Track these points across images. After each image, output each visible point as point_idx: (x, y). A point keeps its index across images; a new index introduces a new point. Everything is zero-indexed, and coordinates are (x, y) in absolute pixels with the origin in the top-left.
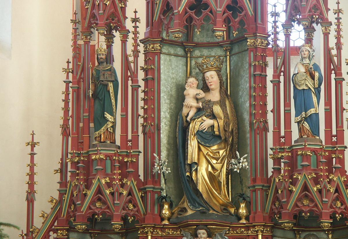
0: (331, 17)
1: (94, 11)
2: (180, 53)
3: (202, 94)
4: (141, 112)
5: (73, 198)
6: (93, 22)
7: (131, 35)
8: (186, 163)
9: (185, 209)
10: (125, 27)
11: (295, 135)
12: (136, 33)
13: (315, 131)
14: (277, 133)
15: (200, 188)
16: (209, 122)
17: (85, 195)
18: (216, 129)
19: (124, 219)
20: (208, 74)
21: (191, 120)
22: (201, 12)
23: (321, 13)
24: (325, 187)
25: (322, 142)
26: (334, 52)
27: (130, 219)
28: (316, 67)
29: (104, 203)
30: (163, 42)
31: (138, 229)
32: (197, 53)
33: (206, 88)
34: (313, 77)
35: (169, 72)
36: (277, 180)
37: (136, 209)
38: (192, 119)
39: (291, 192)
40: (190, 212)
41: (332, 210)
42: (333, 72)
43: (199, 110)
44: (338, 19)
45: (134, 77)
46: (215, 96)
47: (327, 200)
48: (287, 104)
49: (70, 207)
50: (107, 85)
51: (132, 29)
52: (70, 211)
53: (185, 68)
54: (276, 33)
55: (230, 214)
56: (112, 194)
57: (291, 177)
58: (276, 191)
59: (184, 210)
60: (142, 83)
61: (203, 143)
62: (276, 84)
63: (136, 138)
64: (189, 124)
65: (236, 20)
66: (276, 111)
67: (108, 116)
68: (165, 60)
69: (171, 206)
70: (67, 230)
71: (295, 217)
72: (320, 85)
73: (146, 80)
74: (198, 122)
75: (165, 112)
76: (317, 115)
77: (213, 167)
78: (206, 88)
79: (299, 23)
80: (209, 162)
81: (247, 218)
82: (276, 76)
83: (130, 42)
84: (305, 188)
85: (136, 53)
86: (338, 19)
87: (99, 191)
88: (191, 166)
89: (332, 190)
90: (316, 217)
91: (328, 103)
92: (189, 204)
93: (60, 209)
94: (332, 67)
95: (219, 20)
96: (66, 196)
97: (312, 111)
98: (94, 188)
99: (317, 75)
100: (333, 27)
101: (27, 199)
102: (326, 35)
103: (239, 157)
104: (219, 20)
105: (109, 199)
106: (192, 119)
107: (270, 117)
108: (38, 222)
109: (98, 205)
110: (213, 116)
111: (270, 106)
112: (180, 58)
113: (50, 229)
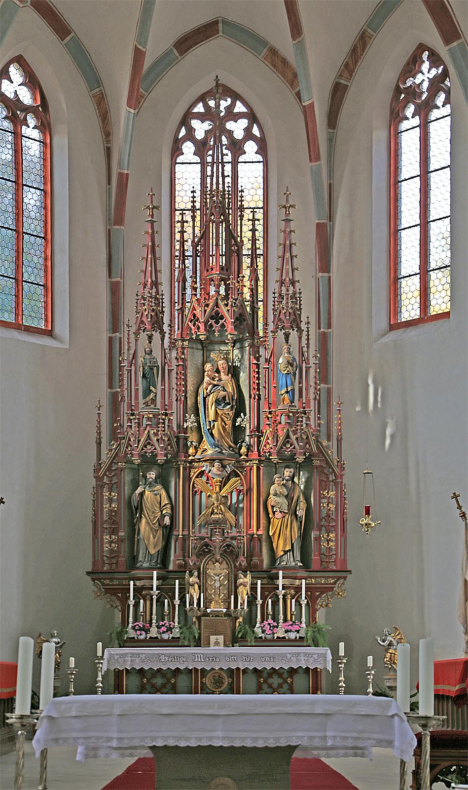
0: (303, 326)
1: (143, 319)
2: (199, 348)
3: (217, 375)
4: (175, 386)
5: (130, 442)
6: (142, 326)
7: (167, 336)
8: (207, 420)
9: (206, 449)
10: (164, 330)
13: (292, 402)
17: (139, 441)
18: (227, 398)
19: (166, 455)
20: (220, 362)
21: (210, 392)
22: (219, 322)
23: (298, 324)
24: (301, 435)
25: (296, 407)
26: (305, 349)
27: (169, 456)
28: (294, 359)
31: (174, 462)
32: (210, 347)
33: (218, 371)
34: (292, 366)
35: (192, 360)
36: (269, 431)
37: (171, 450)
40: (210, 452)
41: (304, 450)
42: (304, 362)
44: (308, 328)
47: (302, 444)
49: (127, 447)
50: (152, 369)
51: (168, 332)
52: (127, 450)
53: (202, 357)
55: (236, 453)
56: (158, 440)
59: (205, 450)
60: (175, 368)
61: (219, 407)
63: (171, 403)
65: (241, 327)
67: (152, 388)
68: (190, 352)
69: (196, 448)
70: (125, 462)
72: (296, 370)
75: (190, 387)
76: (293, 390)
77: (225, 423)
79: (281, 330)
81: (247, 455)
83: (167, 340)
84: (288, 436)
86: (308, 328)
89: (305, 437)
92: (209, 447)
93: (120, 448)
94: (303, 359)
96: (124, 441)
99: (295, 363)
100: (305, 333)
101: (96, 442)
102: (300, 338)
103: (243, 417)
105: (156, 443)
109: (149, 447)
110: (224, 390)
112: (199, 351)
113: (111, 463)
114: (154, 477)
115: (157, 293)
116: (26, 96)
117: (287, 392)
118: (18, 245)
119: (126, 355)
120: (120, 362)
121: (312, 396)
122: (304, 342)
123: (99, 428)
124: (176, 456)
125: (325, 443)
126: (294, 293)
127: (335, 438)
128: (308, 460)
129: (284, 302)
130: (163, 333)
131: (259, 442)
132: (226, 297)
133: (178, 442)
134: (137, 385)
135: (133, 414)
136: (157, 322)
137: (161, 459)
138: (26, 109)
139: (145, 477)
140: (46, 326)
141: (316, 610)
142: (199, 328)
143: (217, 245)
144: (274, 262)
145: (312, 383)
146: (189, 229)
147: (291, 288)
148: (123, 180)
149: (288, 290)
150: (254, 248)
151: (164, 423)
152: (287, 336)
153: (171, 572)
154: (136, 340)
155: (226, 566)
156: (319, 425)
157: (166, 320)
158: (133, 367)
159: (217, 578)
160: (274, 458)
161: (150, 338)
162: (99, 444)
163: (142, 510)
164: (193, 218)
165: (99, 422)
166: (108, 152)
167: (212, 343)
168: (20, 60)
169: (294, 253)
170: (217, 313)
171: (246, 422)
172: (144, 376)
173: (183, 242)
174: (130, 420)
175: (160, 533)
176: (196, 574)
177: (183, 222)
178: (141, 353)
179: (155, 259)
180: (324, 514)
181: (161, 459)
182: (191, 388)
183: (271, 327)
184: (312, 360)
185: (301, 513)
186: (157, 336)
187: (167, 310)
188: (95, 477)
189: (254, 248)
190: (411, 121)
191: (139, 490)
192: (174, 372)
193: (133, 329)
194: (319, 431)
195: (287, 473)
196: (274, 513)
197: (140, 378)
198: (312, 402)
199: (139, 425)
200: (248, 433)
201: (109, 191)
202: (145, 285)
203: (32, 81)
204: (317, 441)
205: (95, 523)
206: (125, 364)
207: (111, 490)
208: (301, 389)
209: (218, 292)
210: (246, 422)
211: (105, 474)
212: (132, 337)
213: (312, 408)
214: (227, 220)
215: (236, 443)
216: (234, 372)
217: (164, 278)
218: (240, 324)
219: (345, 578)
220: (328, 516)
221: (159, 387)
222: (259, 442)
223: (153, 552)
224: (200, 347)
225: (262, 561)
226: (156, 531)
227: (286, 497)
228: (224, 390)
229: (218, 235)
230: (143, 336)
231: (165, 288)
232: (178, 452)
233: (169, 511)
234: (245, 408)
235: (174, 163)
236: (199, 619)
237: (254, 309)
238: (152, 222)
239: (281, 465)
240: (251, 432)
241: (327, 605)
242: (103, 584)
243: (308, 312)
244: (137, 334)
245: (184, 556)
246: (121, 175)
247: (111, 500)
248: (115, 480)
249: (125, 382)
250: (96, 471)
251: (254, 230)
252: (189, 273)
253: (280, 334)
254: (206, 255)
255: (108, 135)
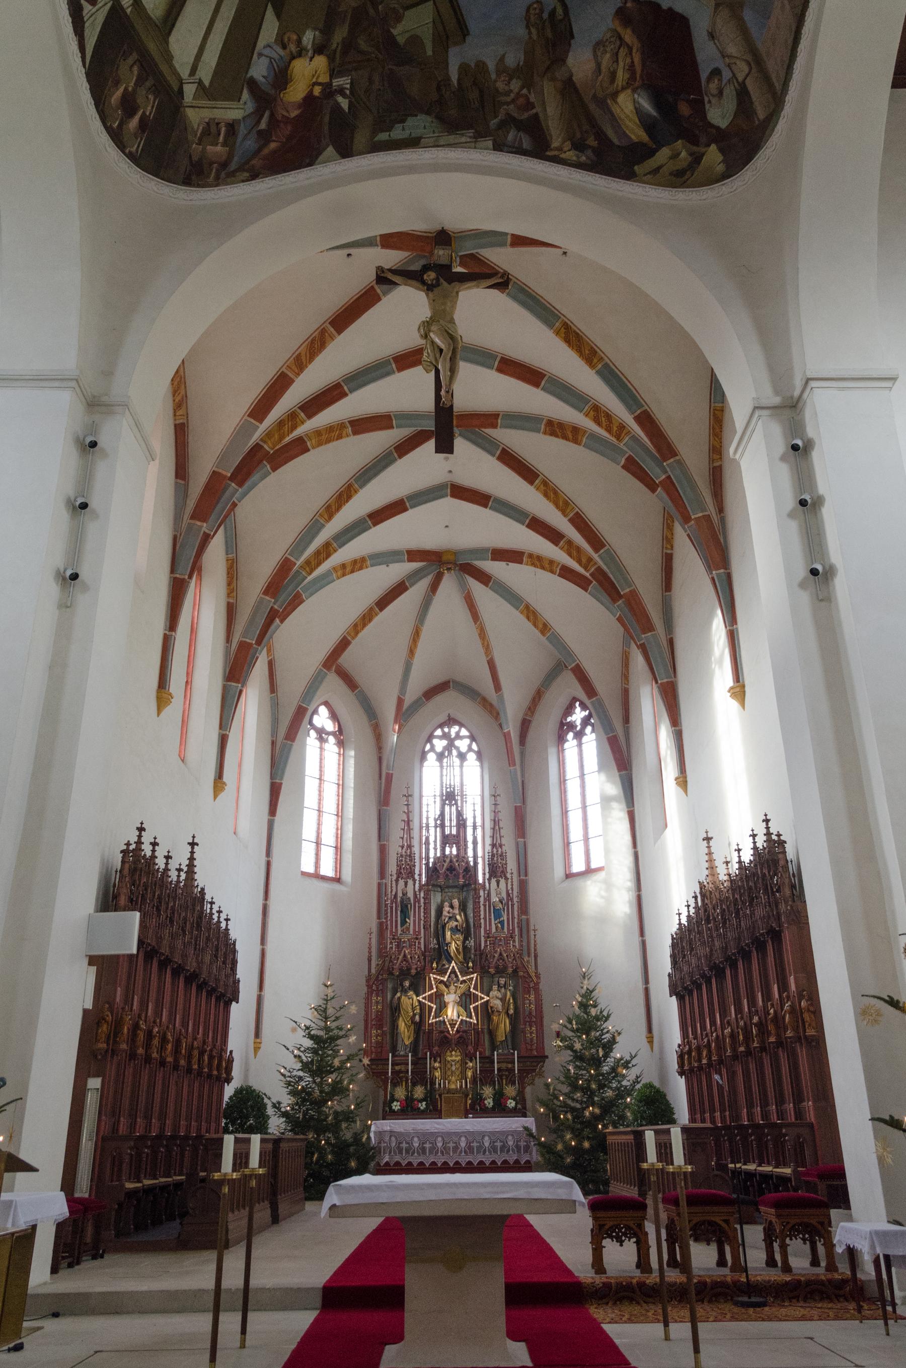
0: (509, 876)
3: (451, 910)
4: (423, 918)
7: (417, 882)
11: (494, 930)
12: (420, 881)
13: (503, 928)
14: (485, 928)
15: (452, 954)
16: (456, 923)
19: (416, 969)
26: (510, 892)
29: (407, 961)
30: (433, 885)
32: (446, 890)
33: (452, 907)
38: (447, 922)
39: (494, 956)
43: (450, 918)
45: (419, 901)
46: (457, 911)
48: (490, 915)
54: (484, 882)
57: (494, 949)
58: (487, 956)
59: (444, 965)
60: (422, 904)
62: (485, 906)
64: (445, 924)
66: (485, 918)
67: (407, 920)
69: (437, 964)
71: (496, 968)
73: (425, 903)
74: (451, 923)
78: (452, 907)
80: (455, 943)
82: (485, 902)
84: (501, 954)
85: (420, 890)
87: (405, 956)
88: (447, 945)
90: (505, 968)
91: (508, 915)
95: (461, 876)
97: (502, 919)
98: (402, 954)
102: (507, 884)
104: (461, 876)
106: (447, 922)
107: (482, 921)
108: (373, 971)
111: (482, 916)
113: (379, 974)
114: (407, 985)
115: (411, 852)
116: (330, 726)
117: (499, 922)
118: (319, 820)
119: (389, 896)
120: (385, 901)
121: (516, 925)
122: (509, 887)
123: (370, 948)
124: (424, 969)
125: (526, 959)
126: (502, 853)
127: (533, 955)
128: (515, 971)
129: (495, 859)
130: (414, 880)
131: (481, 958)
132: (458, 855)
133: (425, 959)
134: (396, 917)
135: (393, 939)
136: (410, 873)
137: (413, 972)
138: (328, 734)
139: (402, 985)
140: (336, 875)
141: (524, 1088)
142: (438, 877)
143: (451, 820)
144: (488, 832)
145: (516, 916)
146: (431, 808)
147: (500, 850)
148: (389, 778)
149: (497, 851)
150: (475, 823)
151: (415, 945)
152: (498, 882)
153: (420, 1059)
154: (397, 885)
155: (459, 1054)
156: (522, 946)
157: (417, 872)
158: (394, 905)
159: (453, 1063)
160: (492, 970)
161: (406, 884)
162: (370, 960)
163: (400, 1010)
164: (435, 802)
165: (370, 945)
166: (380, 759)
167: (448, 887)
168: (326, 704)
169: (501, 826)
170: (451, 866)
171: (471, 943)
172: (401, 912)
173: (427, 818)
174: (391, 943)
175: (412, 1027)
176: (439, 1060)
177: (428, 805)
178: (400, 894)
179: (410, 829)
180: (527, 1013)
181: (413, 972)
182: (433, 919)
183: (487, 876)
184: (515, 900)
185: (511, 1012)
186: (410, 882)
187: (417, 864)
188: (367, 986)
189: (475, 823)
190: (571, 741)
191: (398, 994)
192: (422, 908)
193: (394, 878)
194: (522, 950)
195: (502, 981)
196: (493, 1012)
197: (399, 913)
198: (516, 930)
199: (398, 946)
200: (473, 951)
201: (381, 784)
202: (402, 847)
203: (334, 716)
204: (521, 957)
205: (366, 1021)
206: (389, 902)
207: (377, 996)
208: (508, 919)
209: (451, 852)
210: (471, 943)
211: (373, 983)
212: (394, 883)
213: (517, 933)
214: (456, 804)
215: (465, 958)
216: (463, 908)
217: (415, 843)
218: (467, 874)
219: (544, 1062)
220: (530, 1013)
221: (412, 918)
222: (481, 958)
223: (407, 1043)
224: (439, 890)
225: (485, 1051)
226: (410, 1027)
227: (501, 999)
228: (457, 920)
229: (450, 812)
230: (401, 882)
231: (416, 850)
232: (425, 966)
233: (418, 1011)
234: (471, 934)
235: (421, 766)
236: (440, 1096)
237: (476, 863)
238: (408, 805)
239: (497, 975)
240: (475, 951)
241: (533, 1084)
242: (372, 1069)
243: (511, 865)
244: (397, 881)
245: (429, 1046)
246: (388, 774)
247: (377, 1003)
248: (381, 987)
249: (389, 915)
250: (368, 981)
251: (474, 811)
252: (432, 839)
253: (494, 881)
254: (443, 826)
255: (380, 748)
